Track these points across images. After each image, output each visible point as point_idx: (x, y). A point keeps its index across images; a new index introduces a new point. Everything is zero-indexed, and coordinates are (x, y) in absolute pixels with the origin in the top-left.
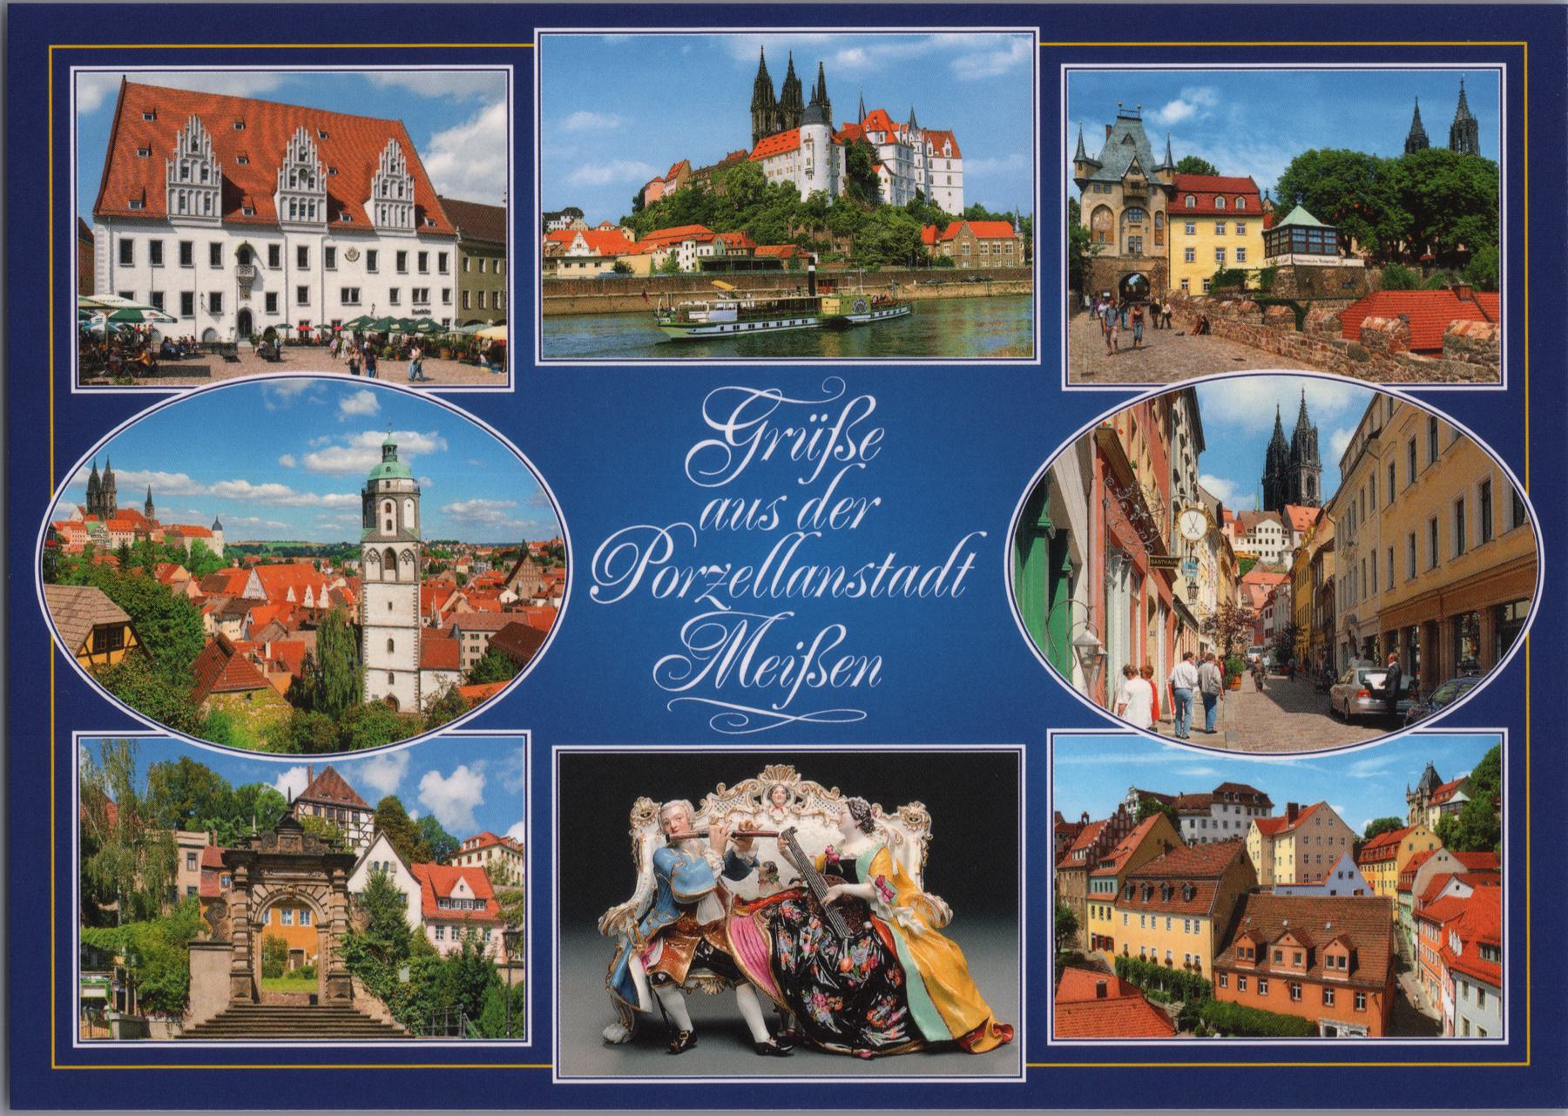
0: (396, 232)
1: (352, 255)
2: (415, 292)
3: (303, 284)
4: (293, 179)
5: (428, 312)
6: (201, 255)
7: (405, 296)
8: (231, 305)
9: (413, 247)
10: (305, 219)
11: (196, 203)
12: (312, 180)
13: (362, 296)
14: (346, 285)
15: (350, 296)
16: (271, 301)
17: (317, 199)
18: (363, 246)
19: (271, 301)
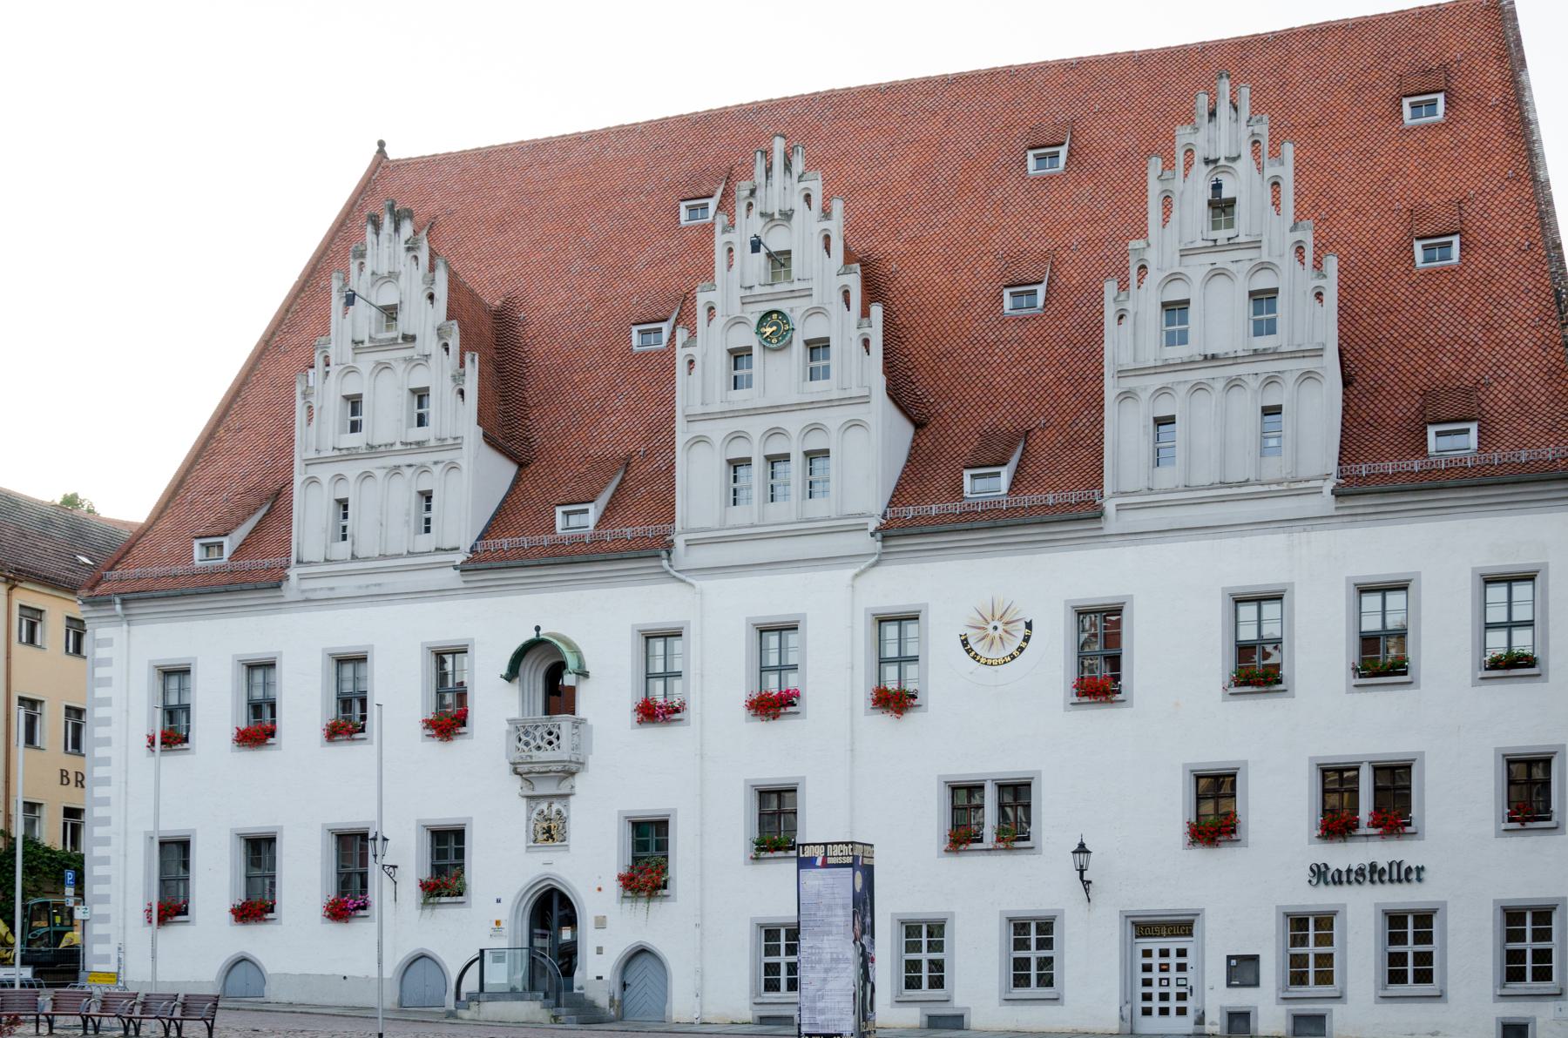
0: (1228, 497)
1: (996, 639)
2: (1336, 781)
3: (775, 774)
4: (739, 356)
5: (1406, 874)
6: (401, 696)
7: (1279, 807)
8: (502, 872)
9: (1323, 567)
10: (786, 510)
11: (383, 509)
12: (818, 347)
13: (1052, 817)
14: (967, 771)
15: (990, 814)
16: (648, 857)
17: (833, 419)
18: (1045, 581)
19: (648, 857)
